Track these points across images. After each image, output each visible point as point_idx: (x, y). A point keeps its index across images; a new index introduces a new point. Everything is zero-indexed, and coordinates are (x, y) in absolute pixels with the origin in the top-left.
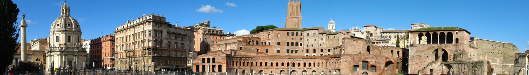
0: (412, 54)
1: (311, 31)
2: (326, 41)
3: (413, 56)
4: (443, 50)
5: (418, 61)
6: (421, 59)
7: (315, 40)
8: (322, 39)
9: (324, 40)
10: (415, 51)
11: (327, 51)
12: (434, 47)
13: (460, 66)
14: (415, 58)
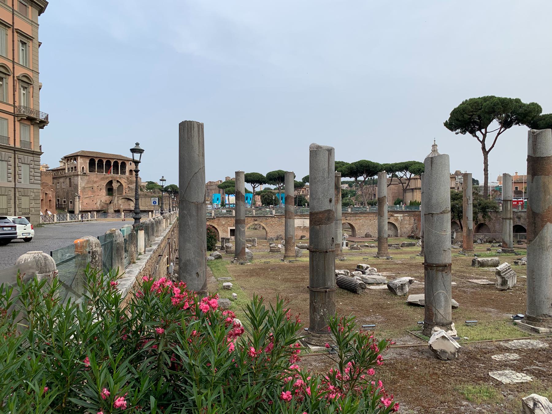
0: (83, 185)
3: (84, 188)
4: (118, 181)
5: (90, 194)
6: (94, 192)
10: (86, 181)
12: (108, 178)
14: (87, 190)
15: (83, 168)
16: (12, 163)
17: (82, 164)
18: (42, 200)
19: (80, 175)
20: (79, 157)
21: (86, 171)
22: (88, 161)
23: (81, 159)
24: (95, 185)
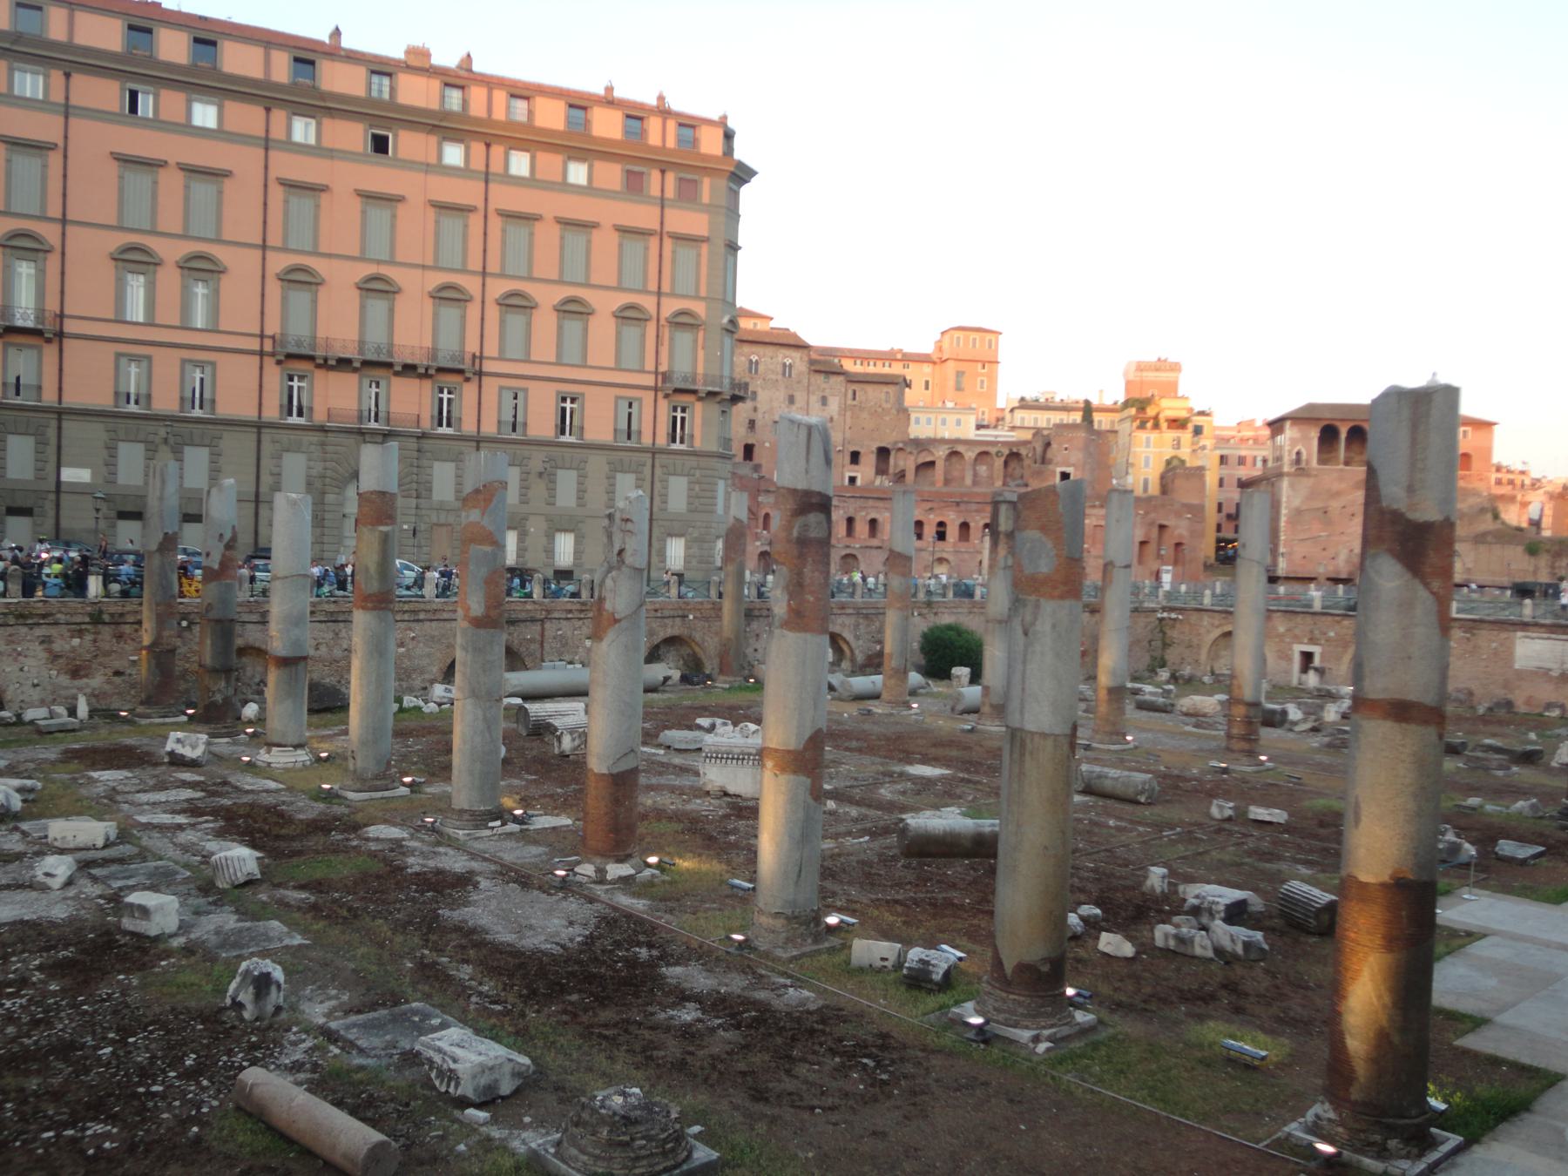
0: (1297, 502)
1: (769, 350)
2: (844, 409)
7: (791, 400)
8: (824, 401)
9: (834, 405)
11: (848, 459)
13: (1497, 550)
15: (1298, 453)
16: (647, 471)
17: (1301, 443)
18: (1143, 543)
19: (1288, 474)
20: (1288, 424)
21: (1308, 462)
22: (1314, 434)
23: (1295, 429)
24: (1335, 505)
